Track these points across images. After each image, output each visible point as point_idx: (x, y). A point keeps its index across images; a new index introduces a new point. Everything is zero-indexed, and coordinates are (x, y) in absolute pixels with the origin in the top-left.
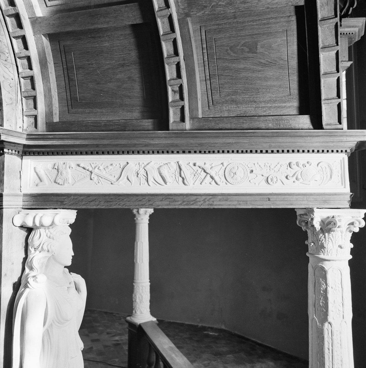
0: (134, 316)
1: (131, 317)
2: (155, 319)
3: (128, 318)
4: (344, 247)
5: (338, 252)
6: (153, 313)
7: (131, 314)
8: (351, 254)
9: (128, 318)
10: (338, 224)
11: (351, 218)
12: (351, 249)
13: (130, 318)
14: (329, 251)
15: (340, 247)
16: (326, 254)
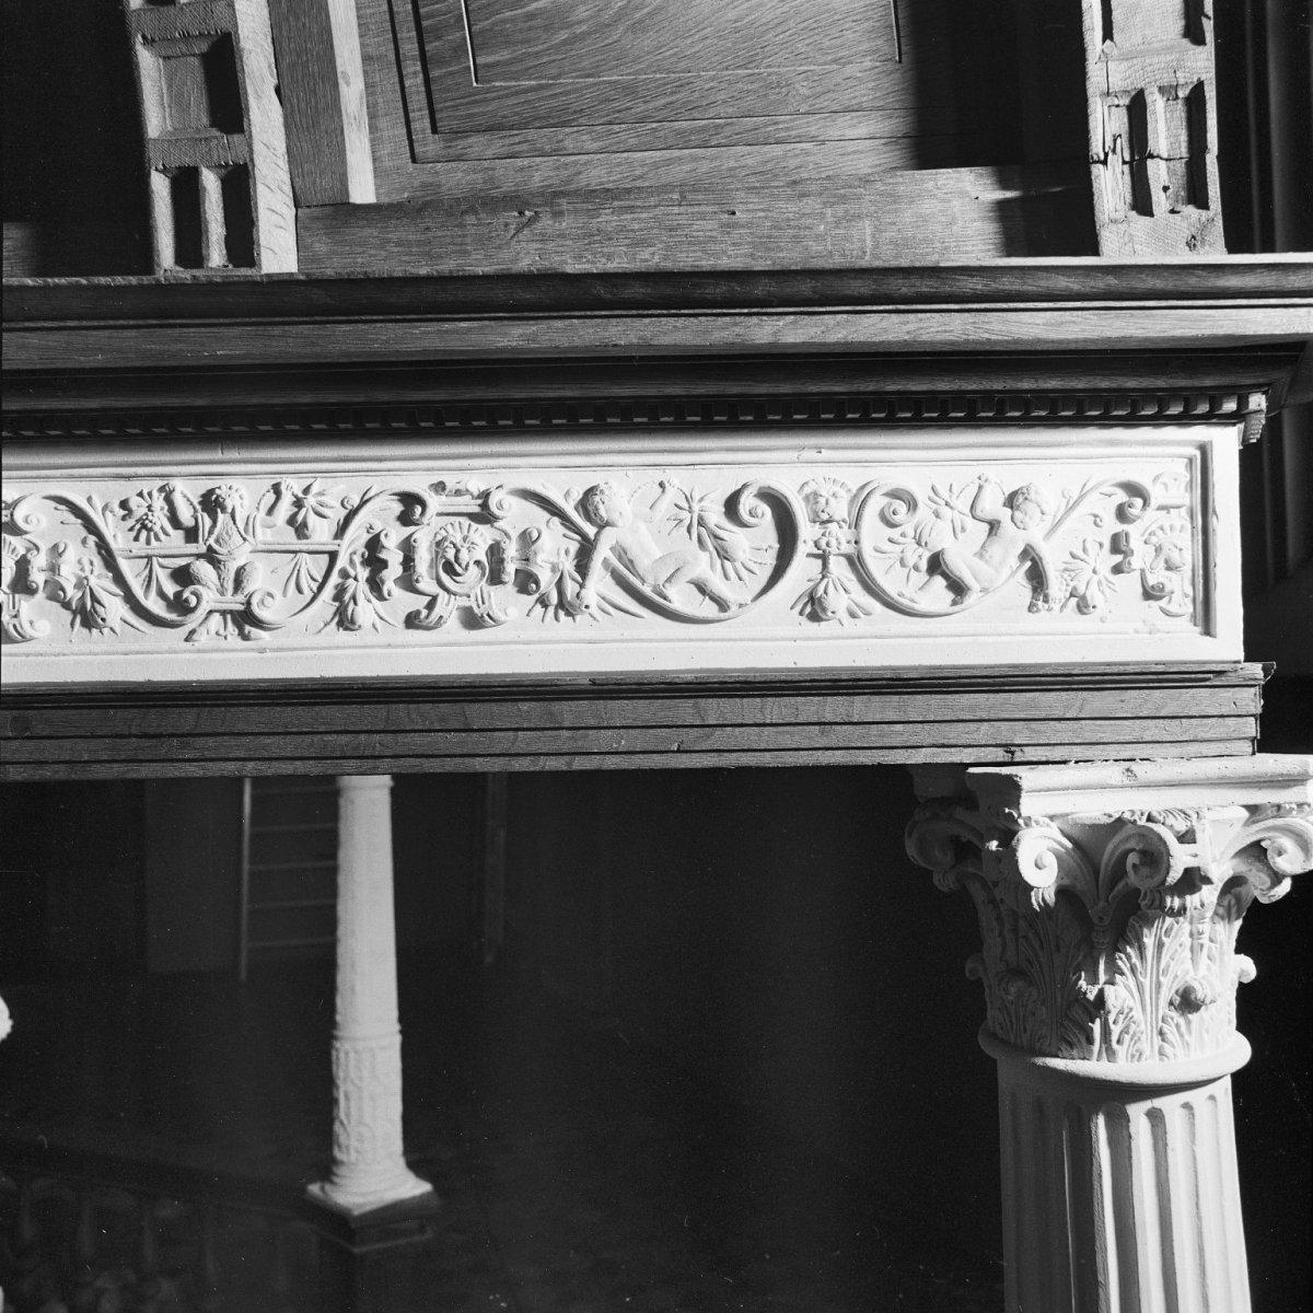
0: (336, 1179)
1: (328, 1187)
2: (424, 1187)
3: (314, 1188)
4: (1207, 1001)
5: (1166, 1029)
6: (418, 1156)
7: (327, 1168)
8: (1241, 1028)
9: (314, 1188)
10: (1181, 859)
11: (1245, 814)
12: (1244, 992)
13: (322, 1189)
14: (1114, 1038)
15: (1187, 1002)
16: (1096, 1047)
